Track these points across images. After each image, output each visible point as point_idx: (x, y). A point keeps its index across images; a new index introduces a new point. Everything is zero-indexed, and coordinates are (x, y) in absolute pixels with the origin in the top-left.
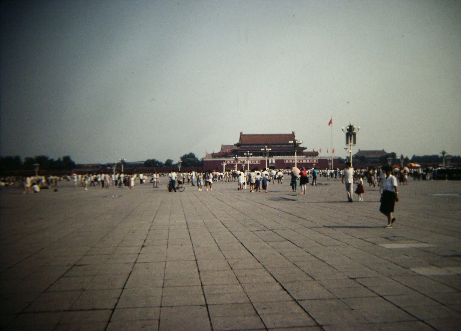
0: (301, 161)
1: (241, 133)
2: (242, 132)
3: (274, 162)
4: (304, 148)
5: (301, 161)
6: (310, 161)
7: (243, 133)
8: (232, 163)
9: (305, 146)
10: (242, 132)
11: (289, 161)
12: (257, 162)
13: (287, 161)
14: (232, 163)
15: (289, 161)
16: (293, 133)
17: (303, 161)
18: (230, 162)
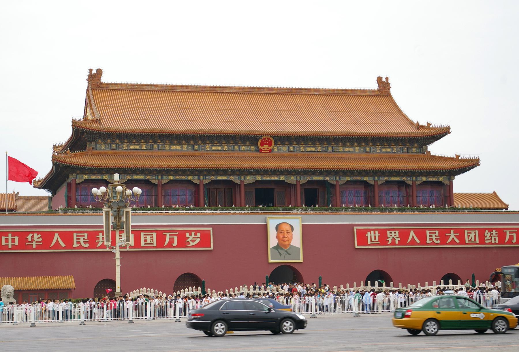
0: (452, 235)
1: (94, 79)
2: (99, 72)
3: (297, 240)
4: (457, 158)
5: (452, 235)
6: (501, 234)
7: (104, 79)
8: (34, 245)
9: (466, 153)
10: (99, 72)
11: (383, 234)
12: (193, 241)
13: (372, 237)
14: (34, 245)
15: (383, 234)
16: (384, 86)
17: (461, 237)
18: (23, 236)
